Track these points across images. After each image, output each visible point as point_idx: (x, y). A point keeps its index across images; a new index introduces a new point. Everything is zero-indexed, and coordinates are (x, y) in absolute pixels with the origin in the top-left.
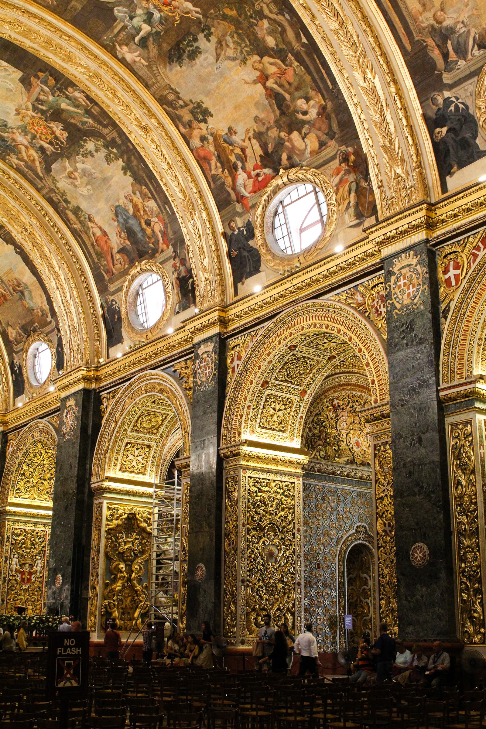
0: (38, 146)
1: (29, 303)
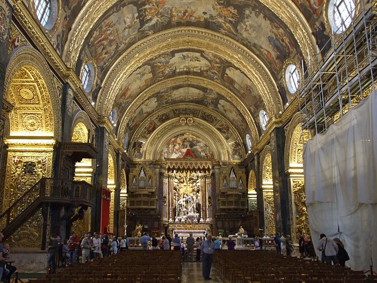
1: (253, 94)
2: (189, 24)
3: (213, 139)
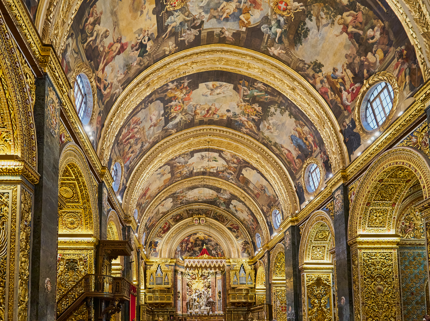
0: (251, 119)
2: (211, 122)
3: (224, 238)
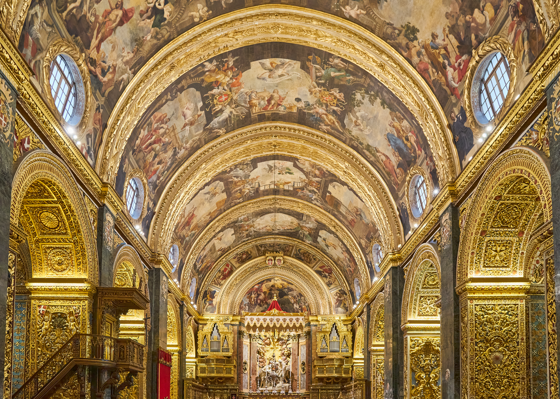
0: (331, 111)
2: (276, 117)
3: (310, 285)
